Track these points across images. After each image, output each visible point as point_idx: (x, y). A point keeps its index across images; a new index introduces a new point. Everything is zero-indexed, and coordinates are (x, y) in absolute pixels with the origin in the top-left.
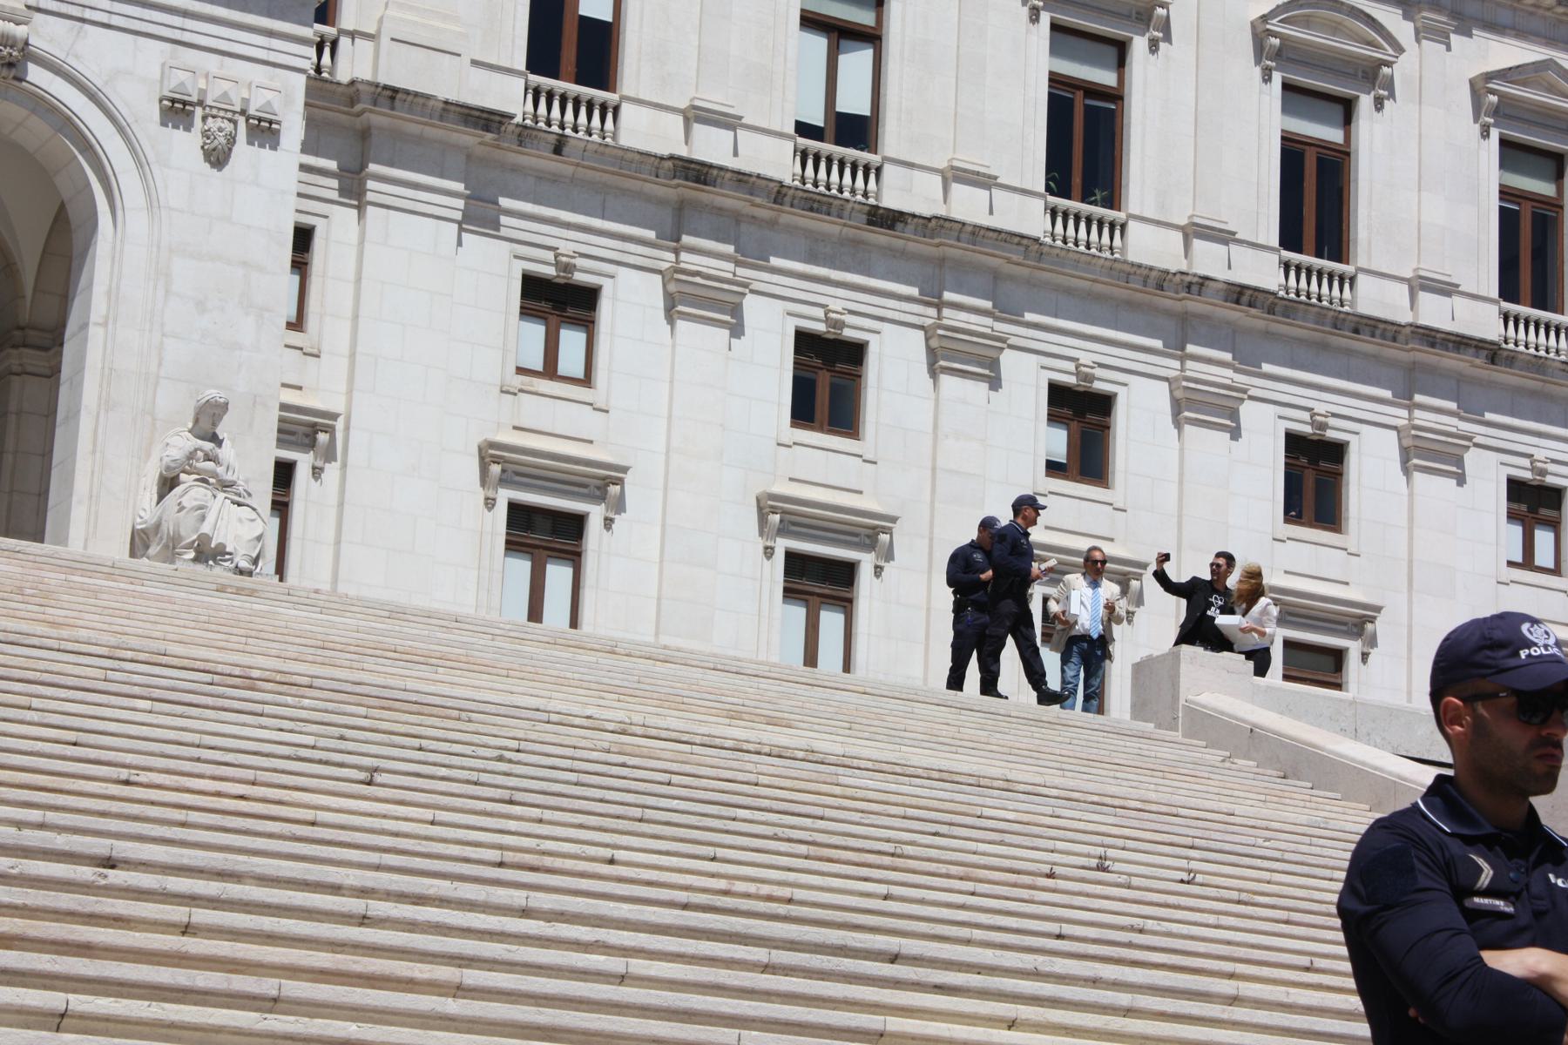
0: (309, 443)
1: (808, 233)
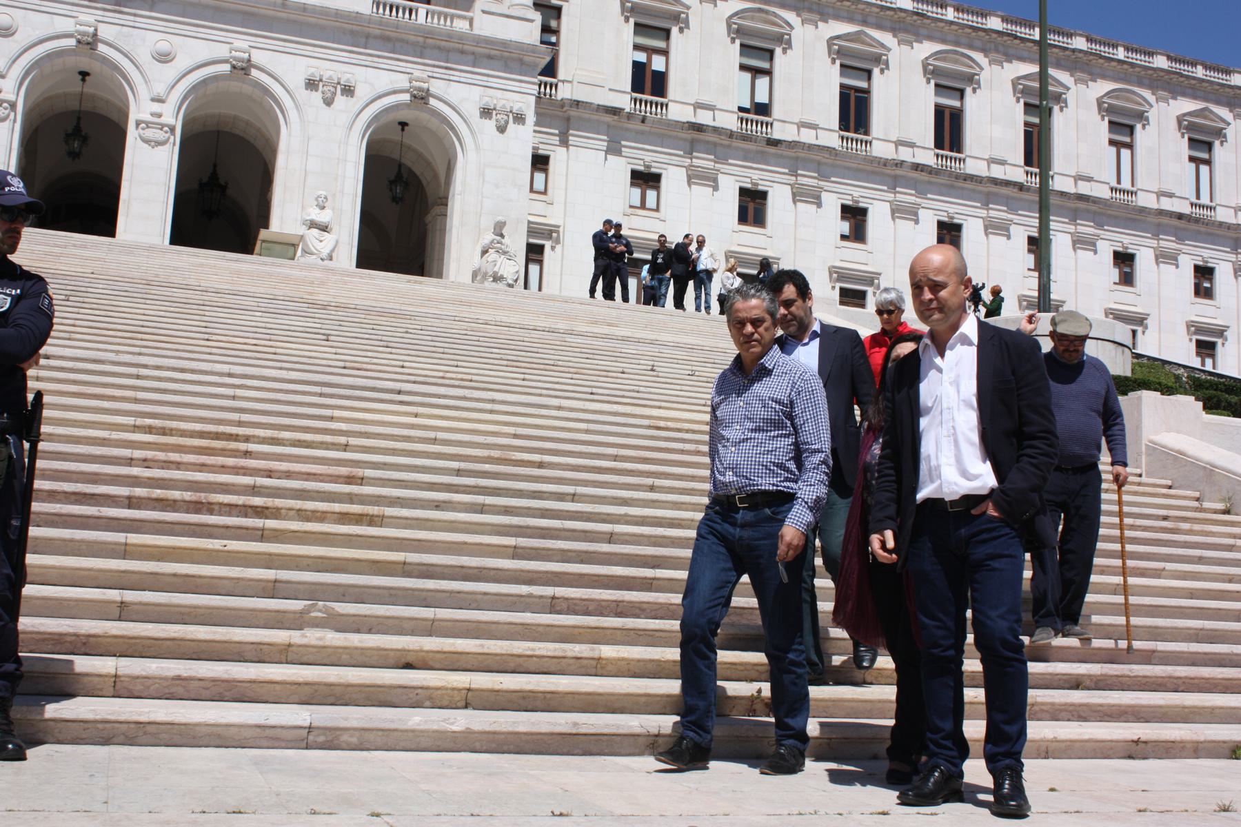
0: (549, 237)
1: (743, 149)
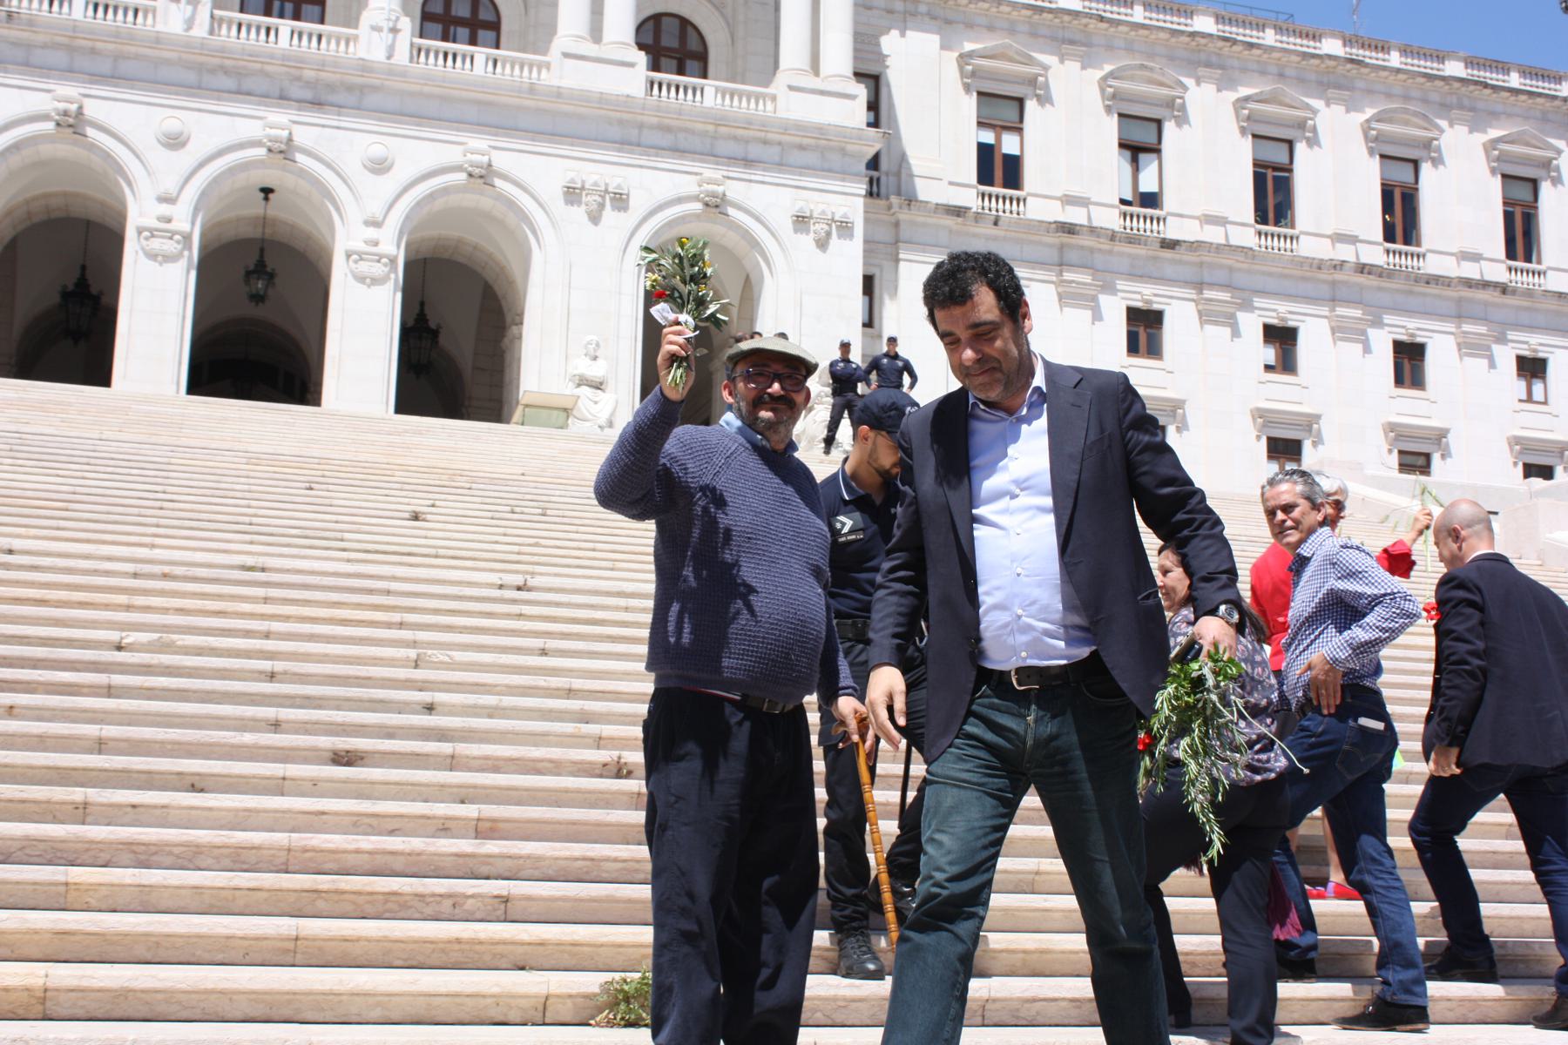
1: (1129, 255)
